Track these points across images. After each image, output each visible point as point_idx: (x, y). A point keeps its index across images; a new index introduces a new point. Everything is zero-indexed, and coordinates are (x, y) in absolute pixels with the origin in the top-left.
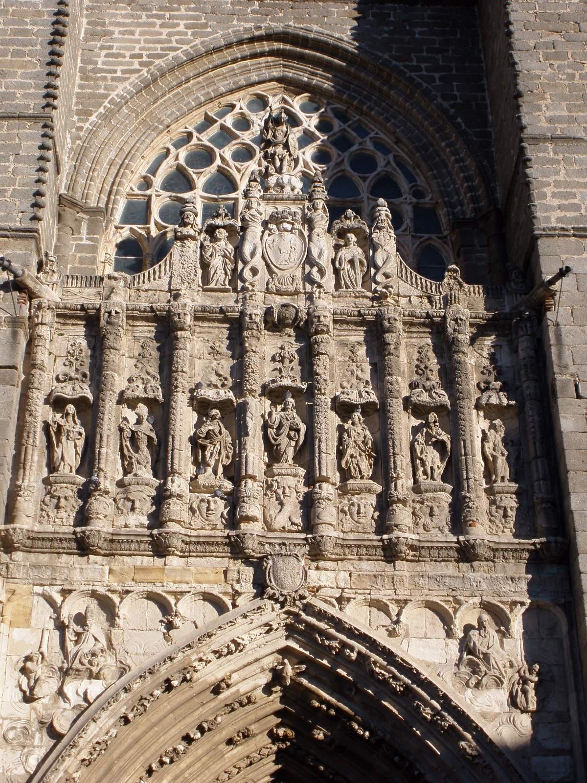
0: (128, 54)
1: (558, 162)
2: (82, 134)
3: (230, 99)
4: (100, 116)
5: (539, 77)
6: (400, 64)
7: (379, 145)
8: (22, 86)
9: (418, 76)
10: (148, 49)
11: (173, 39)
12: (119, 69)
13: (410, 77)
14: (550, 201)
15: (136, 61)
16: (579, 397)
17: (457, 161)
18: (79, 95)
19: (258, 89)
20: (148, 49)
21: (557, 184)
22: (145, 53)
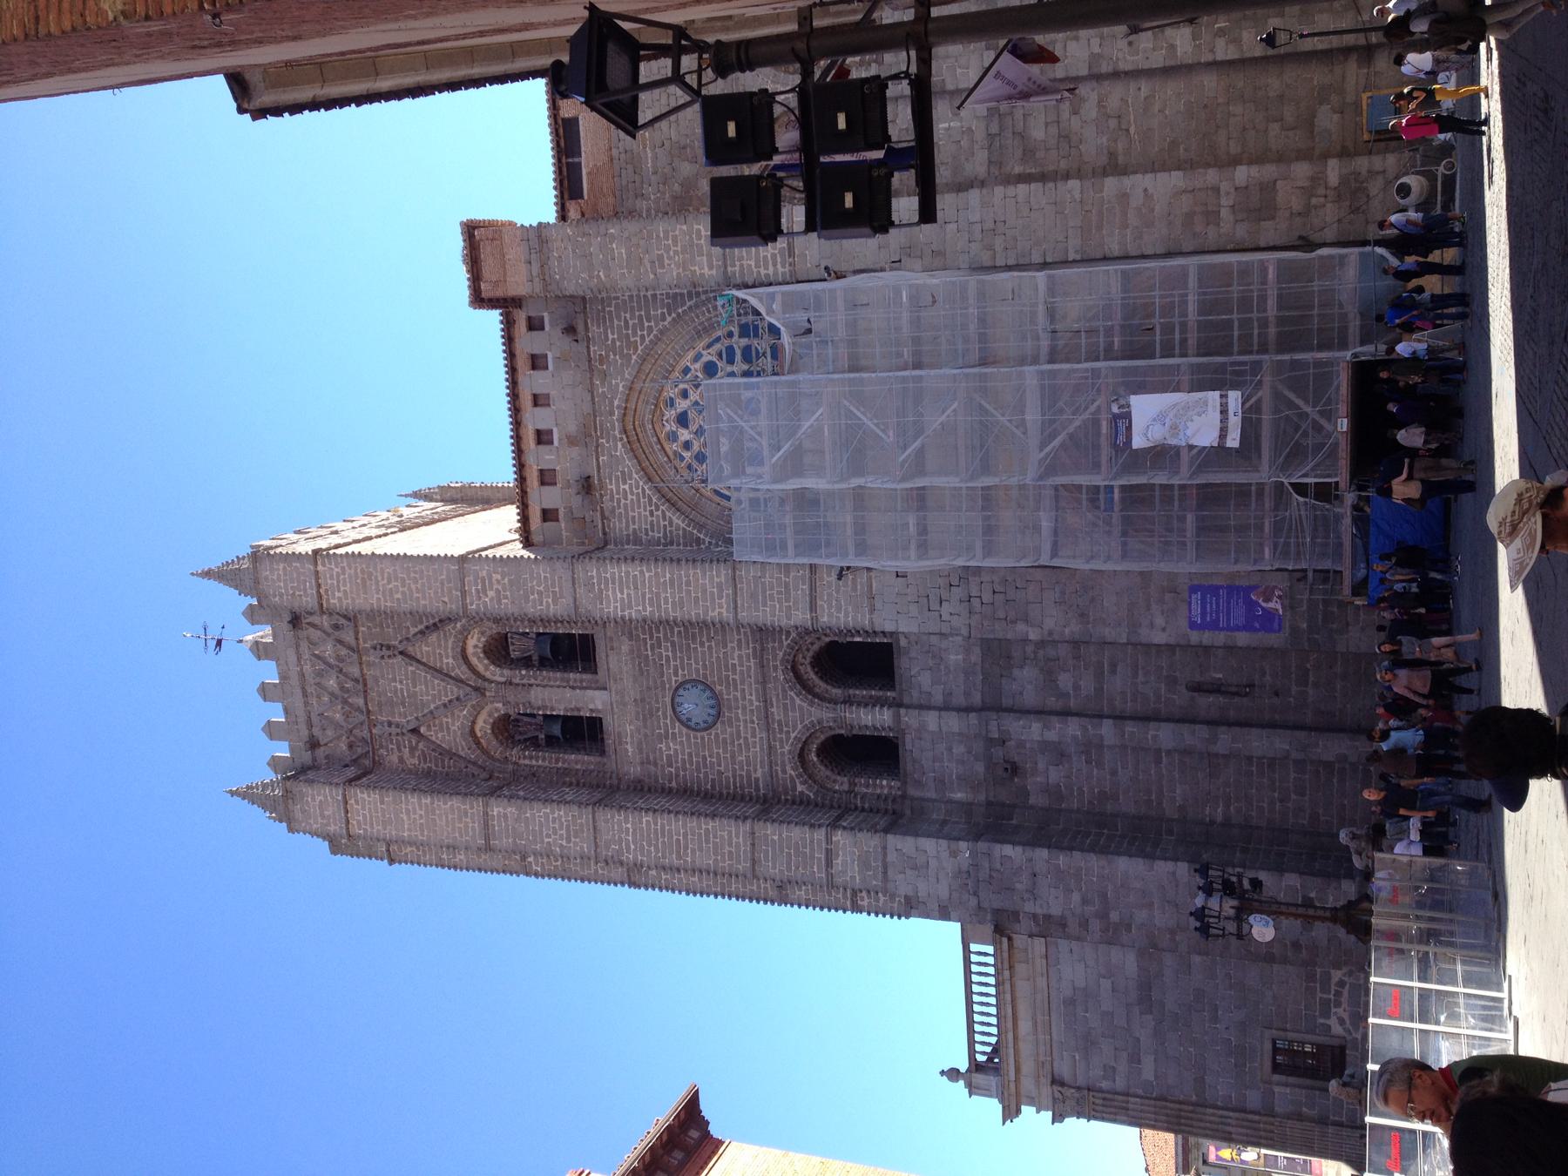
0: (650, 519)
1: (742, 266)
2: (714, 542)
3: (670, 454)
4: (699, 531)
5: (678, 274)
6: (640, 348)
7: (697, 358)
8: (712, 578)
9: (649, 336)
10: (645, 507)
11: (635, 491)
12: (662, 523)
13: (651, 341)
14: (771, 270)
15: (655, 513)
16: (900, 261)
17: (709, 312)
18: (685, 545)
19: (662, 436)
20: (645, 507)
21: (757, 266)
22: (648, 508)
